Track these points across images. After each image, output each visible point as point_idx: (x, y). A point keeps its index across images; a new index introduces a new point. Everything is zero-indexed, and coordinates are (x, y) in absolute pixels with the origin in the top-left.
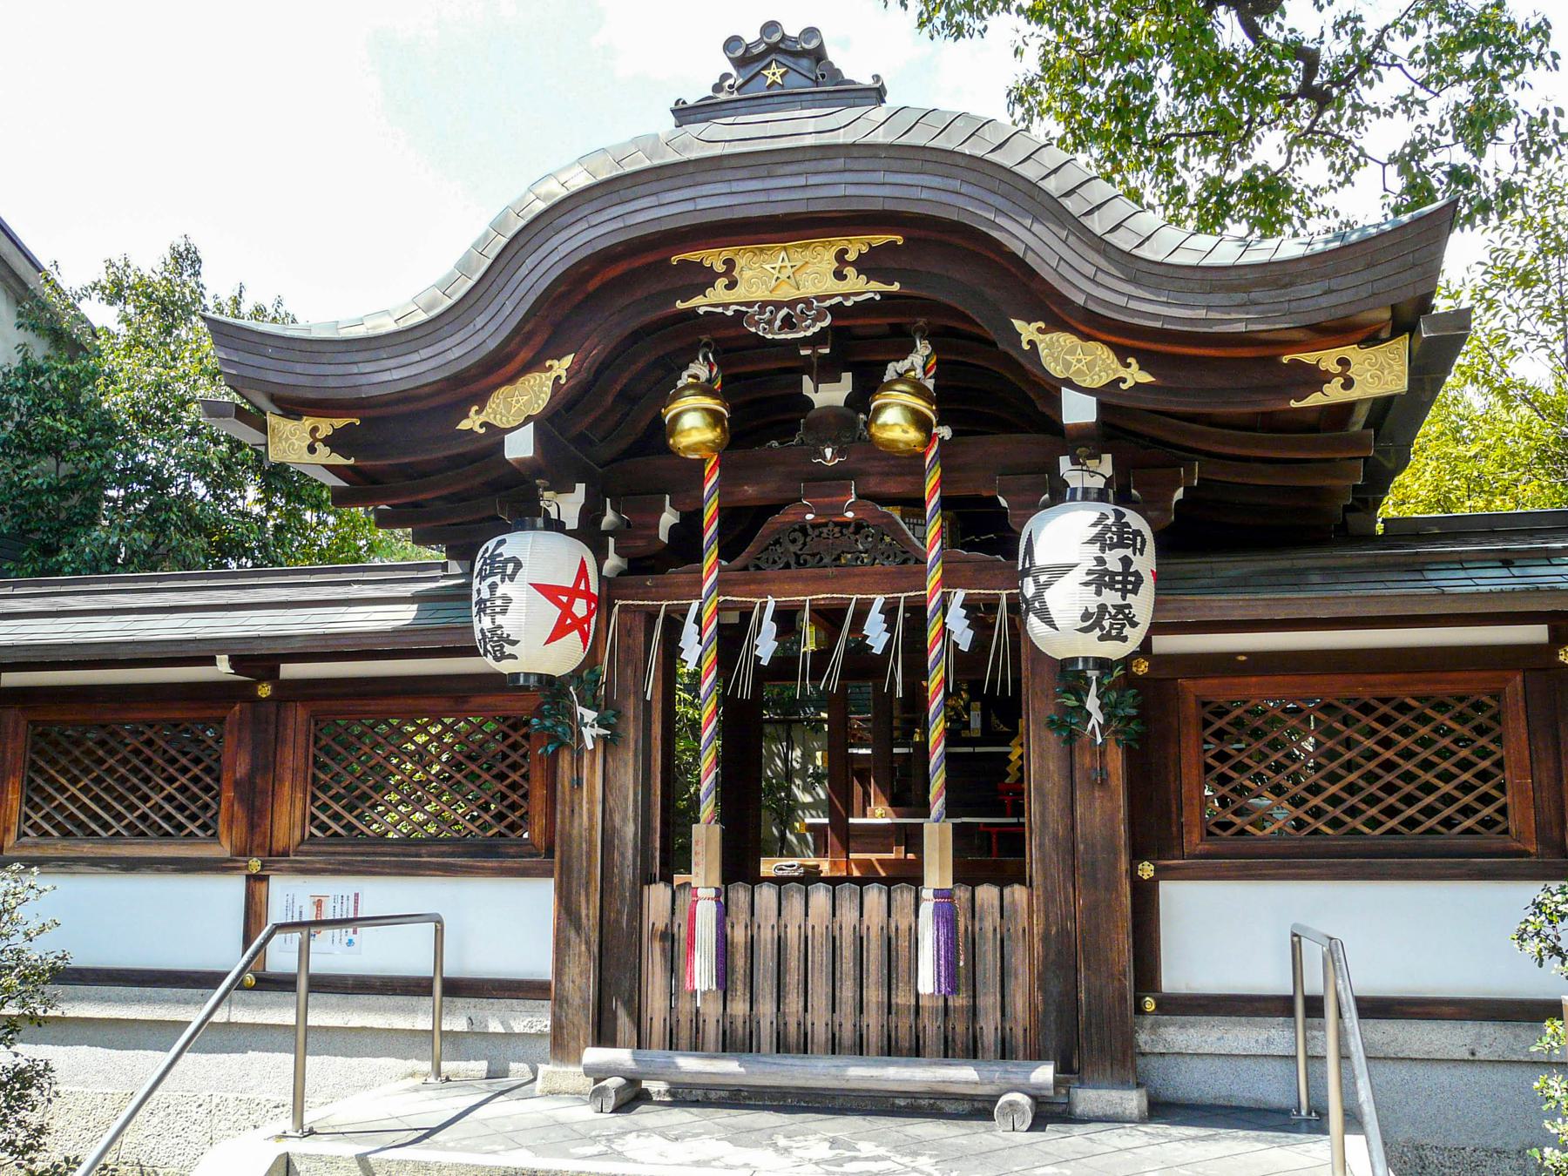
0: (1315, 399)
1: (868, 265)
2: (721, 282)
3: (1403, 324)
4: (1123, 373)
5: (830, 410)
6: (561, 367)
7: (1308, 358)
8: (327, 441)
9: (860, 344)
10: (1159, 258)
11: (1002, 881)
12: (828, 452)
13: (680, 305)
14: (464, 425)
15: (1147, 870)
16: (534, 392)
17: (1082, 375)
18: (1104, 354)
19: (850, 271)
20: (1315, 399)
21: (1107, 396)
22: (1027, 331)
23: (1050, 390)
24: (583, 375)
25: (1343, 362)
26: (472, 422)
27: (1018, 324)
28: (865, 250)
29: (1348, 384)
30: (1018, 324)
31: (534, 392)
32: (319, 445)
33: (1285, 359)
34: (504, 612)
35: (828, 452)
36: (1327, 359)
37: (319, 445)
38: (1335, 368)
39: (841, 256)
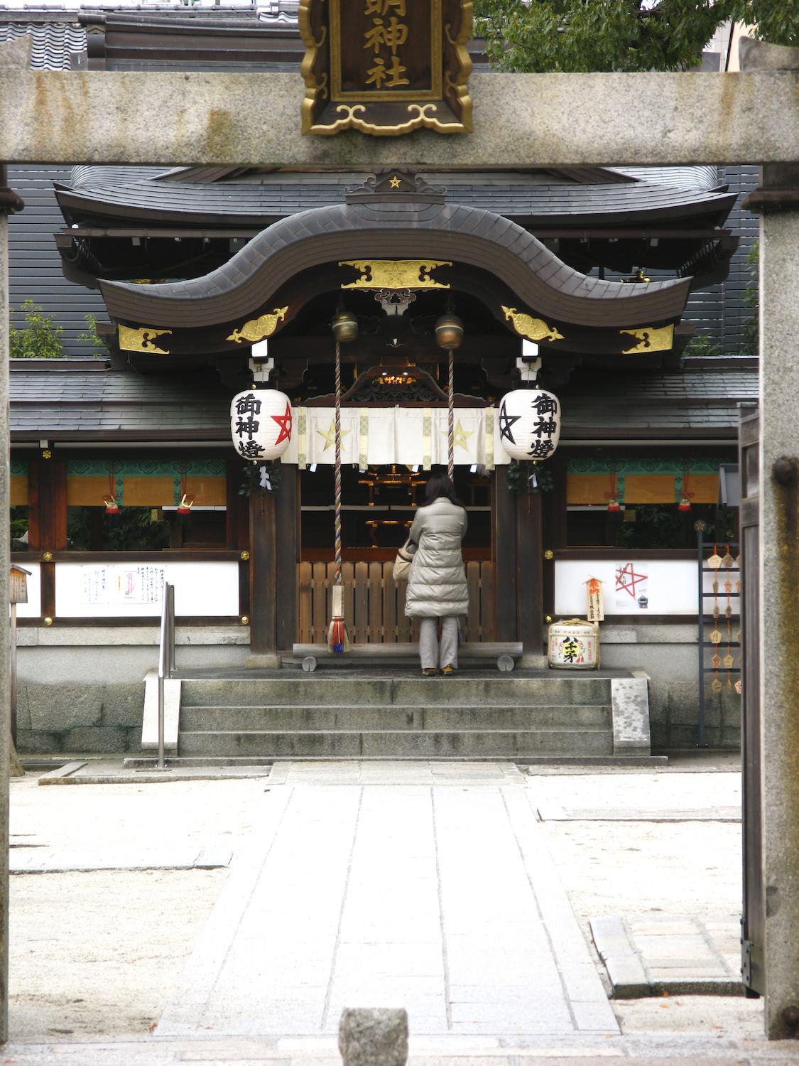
0: (633, 351)
1: (435, 275)
2: (364, 277)
3: (675, 321)
4: (550, 334)
5: (395, 317)
6: (282, 313)
7: (631, 332)
8: (153, 341)
9: (425, 307)
10: (569, 293)
11: (480, 560)
12: (395, 341)
13: (343, 287)
14: (231, 338)
15: (549, 554)
16: (269, 323)
17: (532, 336)
19: (427, 277)
20: (633, 351)
21: (543, 344)
22: (508, 312)
23: (518, 339)
24: (293, 317)
25: (646, 335)
26: (234, 337)
27: (505, 308)
28: (434, 267)
29: (647, 345)
30: (505, 308)
31: (269, 323)
33: (621, 332)
34: (256, 431)
35: (395, 341)
36: (639, 334)
37: (149, 343)
38: (642, 337)
39: (422, 269)
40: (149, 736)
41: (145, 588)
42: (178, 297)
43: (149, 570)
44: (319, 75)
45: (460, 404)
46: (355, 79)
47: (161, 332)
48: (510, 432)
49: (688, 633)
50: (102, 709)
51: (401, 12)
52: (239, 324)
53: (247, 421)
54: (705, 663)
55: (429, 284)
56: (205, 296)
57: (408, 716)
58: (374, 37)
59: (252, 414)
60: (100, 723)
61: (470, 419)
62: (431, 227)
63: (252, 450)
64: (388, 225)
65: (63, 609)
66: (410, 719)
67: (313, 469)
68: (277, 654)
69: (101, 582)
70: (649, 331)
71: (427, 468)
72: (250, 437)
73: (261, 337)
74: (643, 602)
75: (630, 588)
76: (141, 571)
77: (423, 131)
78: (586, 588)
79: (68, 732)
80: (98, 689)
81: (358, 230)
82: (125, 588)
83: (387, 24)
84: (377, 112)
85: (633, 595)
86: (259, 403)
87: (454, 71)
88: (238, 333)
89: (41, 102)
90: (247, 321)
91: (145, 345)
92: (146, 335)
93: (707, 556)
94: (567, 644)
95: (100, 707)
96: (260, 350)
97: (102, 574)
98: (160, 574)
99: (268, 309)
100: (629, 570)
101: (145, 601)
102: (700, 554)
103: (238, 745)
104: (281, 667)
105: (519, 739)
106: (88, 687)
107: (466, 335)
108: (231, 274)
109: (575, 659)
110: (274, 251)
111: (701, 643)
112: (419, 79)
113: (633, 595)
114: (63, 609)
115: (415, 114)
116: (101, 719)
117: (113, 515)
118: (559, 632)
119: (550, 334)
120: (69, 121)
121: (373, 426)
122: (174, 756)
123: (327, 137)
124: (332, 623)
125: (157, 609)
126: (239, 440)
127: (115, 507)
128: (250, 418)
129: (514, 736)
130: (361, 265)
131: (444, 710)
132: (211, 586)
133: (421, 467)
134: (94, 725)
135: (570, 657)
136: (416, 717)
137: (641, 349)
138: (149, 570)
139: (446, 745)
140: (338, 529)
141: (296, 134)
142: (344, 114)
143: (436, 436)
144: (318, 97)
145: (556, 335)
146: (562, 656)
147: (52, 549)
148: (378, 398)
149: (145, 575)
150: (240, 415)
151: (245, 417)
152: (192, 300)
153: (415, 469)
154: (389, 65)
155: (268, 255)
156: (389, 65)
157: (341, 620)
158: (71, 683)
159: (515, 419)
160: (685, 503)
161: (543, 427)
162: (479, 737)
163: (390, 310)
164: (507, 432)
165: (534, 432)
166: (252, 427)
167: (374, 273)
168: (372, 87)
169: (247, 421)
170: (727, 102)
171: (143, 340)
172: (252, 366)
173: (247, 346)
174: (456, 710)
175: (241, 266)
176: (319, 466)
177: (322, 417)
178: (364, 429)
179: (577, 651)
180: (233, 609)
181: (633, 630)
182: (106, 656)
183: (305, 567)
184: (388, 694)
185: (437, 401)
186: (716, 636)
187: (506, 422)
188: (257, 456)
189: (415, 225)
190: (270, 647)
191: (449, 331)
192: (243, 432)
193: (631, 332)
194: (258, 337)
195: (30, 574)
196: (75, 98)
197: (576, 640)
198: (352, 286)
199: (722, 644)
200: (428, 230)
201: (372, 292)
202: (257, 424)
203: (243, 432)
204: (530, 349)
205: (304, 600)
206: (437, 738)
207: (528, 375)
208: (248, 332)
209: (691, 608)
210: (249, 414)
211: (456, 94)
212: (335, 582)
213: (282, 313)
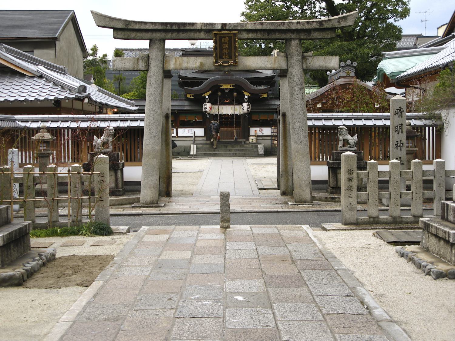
3: (267, 93)
6: (210, 92)
16: (208, 93)
21: (248, 96)
22: (243, 92)
23: (245, 95)
26: (204, 95)
31: (208, 93)
40: (191, 153)
44: (216, 57)
45: (236, 105)
46: (221, 58)
49: (269, 138)
51: (228, 48)
52: (204, 94)
55: (232, 87)
58: (224, 51)
60: (184, 151)
61: (238, 107)
65: (179, 135)
74: (263, 134)
77: (231, 65)
78: (254, 132)
79: (180, 153)
83: (226, 50)
84: (224, 62)
87: (235, 56)
89: (176, 61)
93: (272, 127)
96: (207, 97)
107: (237, 95)
108: (203, 86)
111: (271, 139)
112: (230, 57)
114: (179, 135)
115: (230, 62)
118: (251, 138)
120: (180, 64)
121: (223, 108)
122: (195, 156)
123: (217, 66)
125: (193, 135)
126: (204, 110)
130: (222, 85)
132: (200, 132)
137: (262, 97)
139: (234, 154)
141: (213, 65)
142: (220, 63)
144: (216, 60)
145: (250, 95)
151: (205, 107)
154: (226, 55)
156: (226, 55)
160: (269, 119)
161: (248, 108)
162: (239, 153)
163: (226, 91)
166: (206, 108)
168: (224, 59)
170: (275, 61)
172: (206, 99)
173: (205, 97)
175: (204, 85)
177: (216, 107)
178: (222, 109)
180: (203, 135)
185: (233, 104)
191: (235, 94)
196: (181, 61)
201: (223, 89)
204: (246, 97)
206: (233, 153)
207: (246, 101)
208: (205, 95)
209: (269, 134)
211: (236, 60)
213: (210, 92)
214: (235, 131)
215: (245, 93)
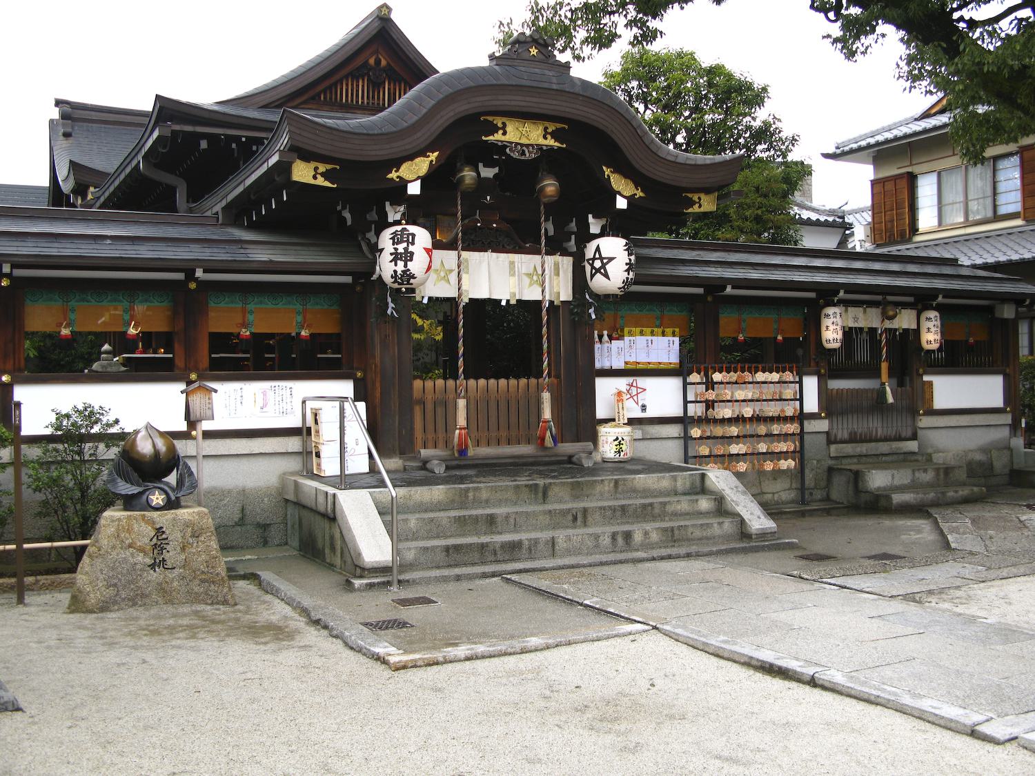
1: (555, 135)
2: (501, 132)
4: (636, 192)
5: (487, 179)
6: (433, 156)
7: (690, 195)
8: (322, 174)
12: (488, 198)
13: (484, 138)
14: (390, 176)
16: (422, 165)
18: (632, 185)
19: (549, 137)
21: (630, 199)
22: (607, 171)
23: (613, 194)
24: (443, 161)
26: (393, 175)
31: (422, 165)
32: (319, 176)
34: (411, 260)
35: (488, 198)
37: (319, 176)
41: (277, 403)
42: (357, 131)
43: (280, 388)
47: (329, 167)
48: (605, 270)
49: (674, 430)
50: (243, 509)
52: (397, 163)
53: (403, 251)
54: (690, 450)
55: (551, 142)
56: (380, 132)
57: (573, 515)
59: (408, 245)
60: (242, 522)
62: (567, 90)
63: (405, 278)
64: (535, 84)
66: (575, 519)
67: (425, 301)
68: (400, 458)
69: (239, 398)
70: (703, 196)
71: (513, 302)
72: (406, 266)
73: (416, 177)
74: (644, 408)
75: (635, 398)
76: (273, 389)
78: (614, 399)
80: (238, 493)
81: (512, 85)
82: (260, 403)
85: (637, 404)
86: (413, 235)
88: (396, 171)
90: (404, 162)
91: (315, 177)
92: (316, 169)
93: (689, 374)
94: (617, 443)
95: (241, 508)
97: (240, 391)
98: (289, 391)
99: (422, 153)
100: (635, 384)
101: (277, 414)
102: (685, 373)
103: (447, 556)
104: (405, 469)
105: (676, 532)
106: (229, 492)
109: (622, 454)
110: (441, 96)
111: (686, 438)
113: (637, 404)
116: (242, 519)
117: (246, 340)
118: (607, 434)
119: (636, 192)
124: (457, 432)
127: (248, 333)
128: (406, 249)
129: (672, 529)
130: (499, 121)
131: (600, 508)
133: (508, 301)
134: (237, 524)
135: (619, 452)
136: (579, 516)
138: (280, 388)
140: (461, 352)
143: (519, 276)
145: (640, 194)
146: (613, 451)
147: (196, 370)
148: (473, 244)
149: (277, 391)
150: (395, 246)
151: (401, 248)
152: (368, 135)
153: (504, 303)
155: (437, 100)
157: (464, 429)
158: (215, 488)
159: (611, 259)
164: (602, 271)
165: (626, 271)
167: (509, 129)
169: (403, 251)
171: (313, 173)
173: (404, 183)
174: (610, 507)
176: (430, 298)
179: (624, 447)
181: (640, 429)
182: (245, 464)
183: (418, 384)
184: (540, 495)
186: (696, 432)
187: (602, 262)
188: (408, 283)
189: (555, 87)
190: (395, 453)
192: (399, 262)
193: (690, 195)
194: (413, 176)
195: (216, 391)
197: (623, 439)
198: (491, 138)
199: (701, 438)
200: (565, 91)
202: (412, 254)
203: (399, 262)
205: (418, 411)
209: (677, 411)
210: (405, 245)
212: (458, 396)
213: (433, 156)
214: (546, 396)
215: (618, 183)
